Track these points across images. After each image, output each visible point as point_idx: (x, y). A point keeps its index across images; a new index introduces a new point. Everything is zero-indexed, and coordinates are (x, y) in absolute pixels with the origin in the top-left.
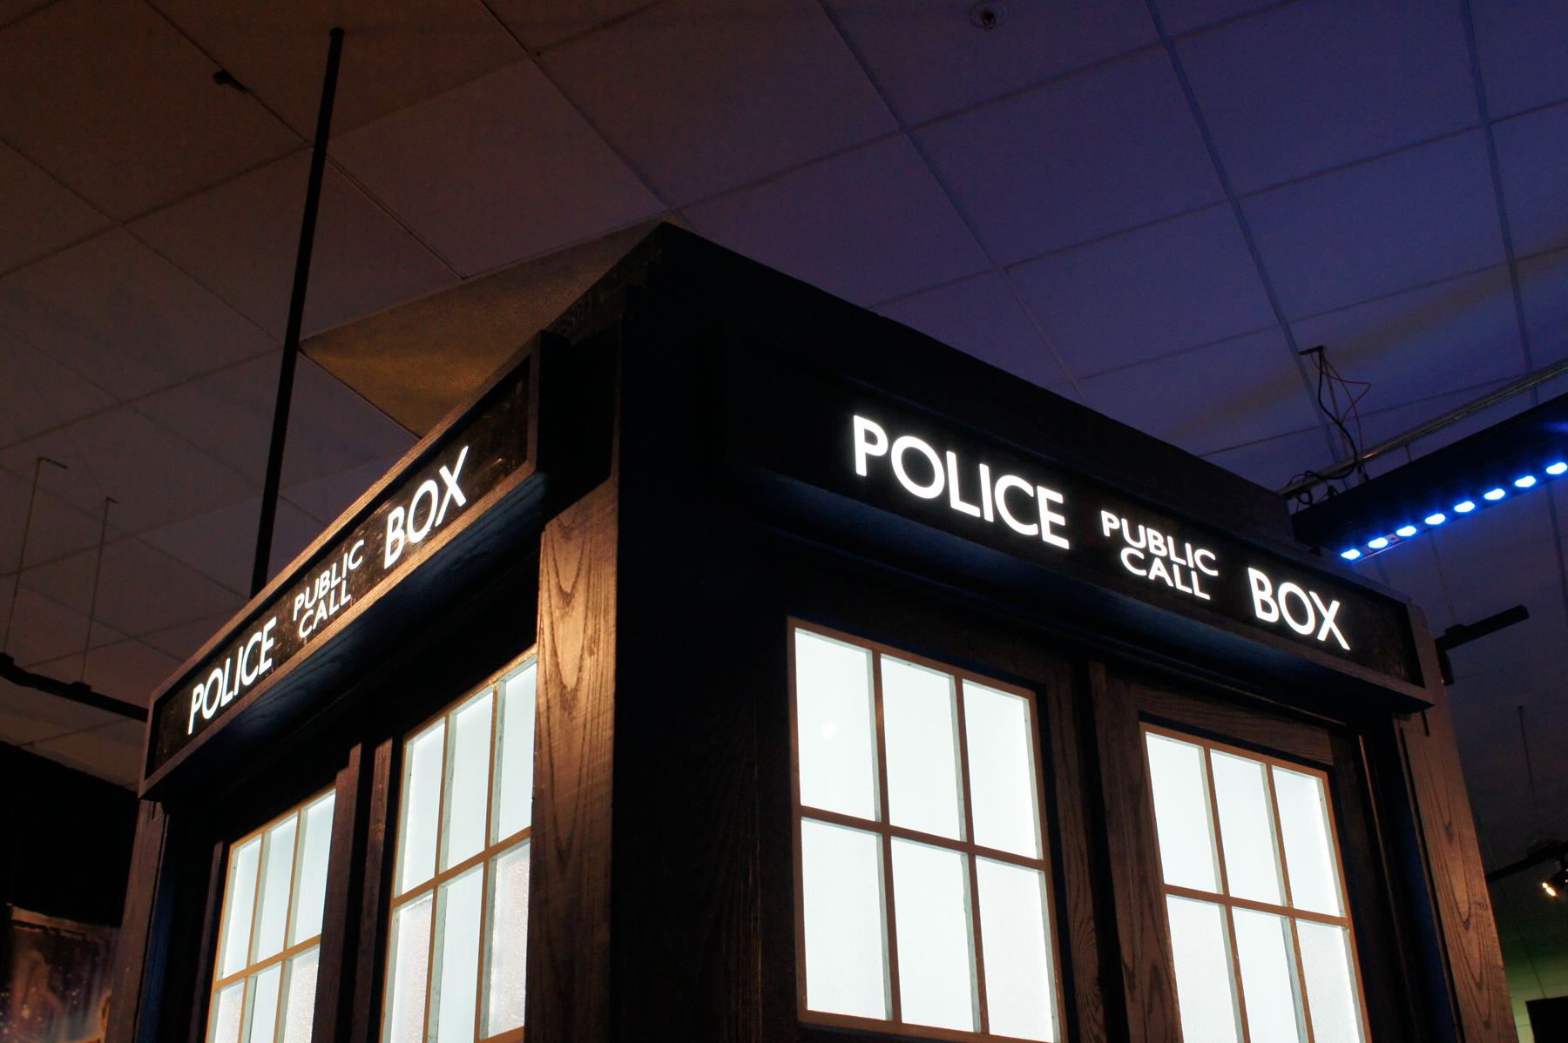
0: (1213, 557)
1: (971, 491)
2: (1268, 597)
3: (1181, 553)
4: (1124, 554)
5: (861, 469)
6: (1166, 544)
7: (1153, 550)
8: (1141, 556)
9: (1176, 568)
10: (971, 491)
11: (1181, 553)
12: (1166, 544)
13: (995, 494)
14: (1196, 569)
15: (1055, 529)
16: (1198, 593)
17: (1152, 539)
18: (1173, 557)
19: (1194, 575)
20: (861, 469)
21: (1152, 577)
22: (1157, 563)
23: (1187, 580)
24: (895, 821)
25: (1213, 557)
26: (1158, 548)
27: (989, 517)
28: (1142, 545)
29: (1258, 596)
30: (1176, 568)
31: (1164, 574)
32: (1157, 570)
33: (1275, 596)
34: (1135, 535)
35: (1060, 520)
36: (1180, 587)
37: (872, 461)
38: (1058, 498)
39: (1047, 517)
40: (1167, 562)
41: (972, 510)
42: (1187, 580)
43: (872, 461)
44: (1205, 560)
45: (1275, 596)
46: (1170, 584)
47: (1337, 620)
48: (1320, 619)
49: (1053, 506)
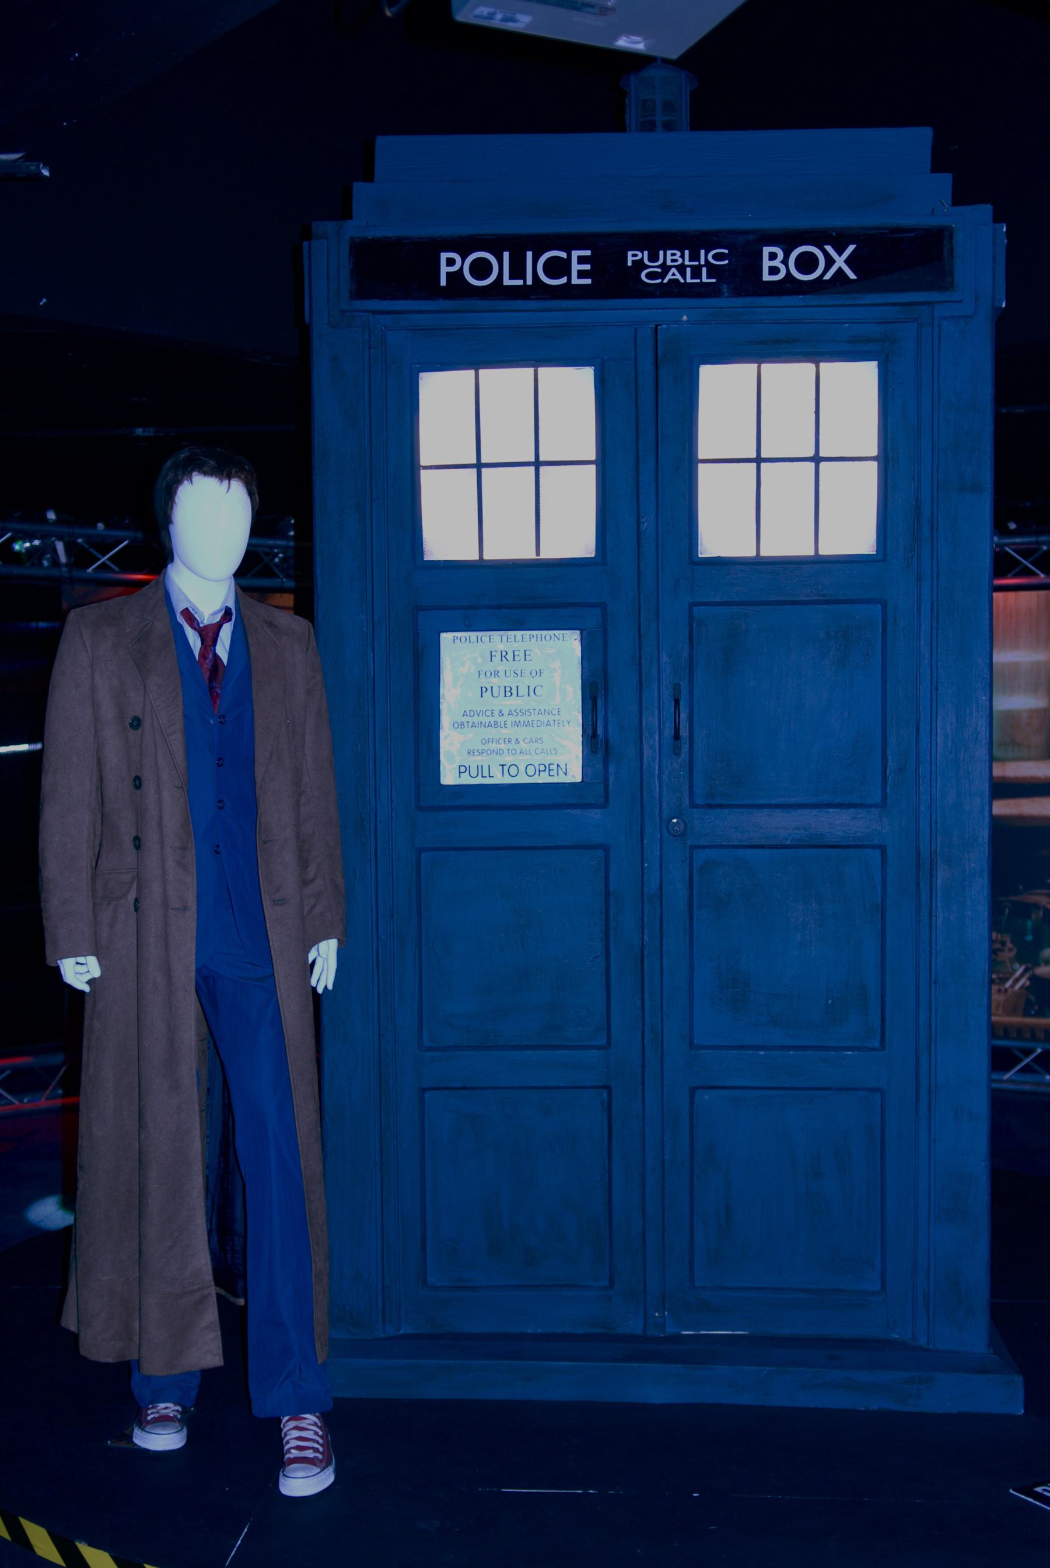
1: (517, 271)
3: (694, 257)
6: (683, 256)
7: (669, 263)
8: (659, 270)
9: (688, 270)
10: (517, 271)
11: (694, 257)
12: (683, 256)
13: (535, 267)
16: (705, 280)
17: (671, 256)
19: (704, 270)
21: (665, 281)
22: (674, 270)
23: (696, 272)
26: (673, 261)
27: (529, 282)
28: (661, 261)
29: (766, 264)
30: (688, 270)
31: (678, 276)
32: (673, 275)
33: (785, 262)
34: (653, 258)
36: (689, 280)
37: (448, 274)
38: (588, 253)
39: (575, 267)
40: (681, 269)
42: (696, 272)
43: (448, 274)
45: (785, 262)
46: (682, 281)
49: (581, 260)
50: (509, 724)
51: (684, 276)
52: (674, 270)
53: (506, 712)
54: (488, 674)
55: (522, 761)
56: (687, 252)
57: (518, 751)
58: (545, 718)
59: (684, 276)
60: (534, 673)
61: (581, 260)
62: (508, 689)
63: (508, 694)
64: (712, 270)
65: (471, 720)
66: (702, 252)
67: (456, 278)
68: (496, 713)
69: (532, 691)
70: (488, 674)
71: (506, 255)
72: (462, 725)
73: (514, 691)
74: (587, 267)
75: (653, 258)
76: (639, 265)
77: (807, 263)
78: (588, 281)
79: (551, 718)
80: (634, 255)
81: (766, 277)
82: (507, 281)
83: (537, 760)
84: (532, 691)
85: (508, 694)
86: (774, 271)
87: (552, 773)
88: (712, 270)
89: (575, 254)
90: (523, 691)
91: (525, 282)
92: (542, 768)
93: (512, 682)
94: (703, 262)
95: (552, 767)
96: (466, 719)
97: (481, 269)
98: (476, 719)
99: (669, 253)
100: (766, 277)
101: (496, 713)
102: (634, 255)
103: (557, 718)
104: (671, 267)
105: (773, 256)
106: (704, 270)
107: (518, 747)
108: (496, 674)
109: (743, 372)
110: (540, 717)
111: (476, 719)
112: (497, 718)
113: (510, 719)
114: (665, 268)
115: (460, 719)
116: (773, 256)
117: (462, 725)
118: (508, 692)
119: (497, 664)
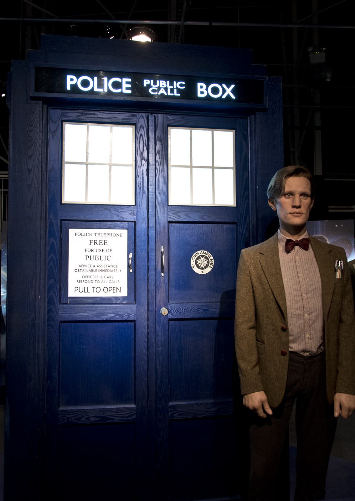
0: (184, 83)
1: (100, 85)
2: (203, 90)
3: (172, 84)
4: (150, 91)
5: (69, 88)
6: (166, 84)
7: (161, 86)
8: (157, 89)
9: (169, 90)
10: (100, 85)
12: (166, 84)
13: (108, 84)
14: (177, 88)
15: (127, 89)
17: (162, 83)
18: (169, 86)
19: (175, 90)
20: (69, 88)
21: (159, 94)
22: (162, 89)
24: (211, 170)
25: (184, 83)
27: (106, 90)
28: (157, 86)
29: (199, 90)
30: (169, 90)
32: (162, 91)
33: (207, 89)
34: (155, 83)
35: (129, 86)
36: (169, 94)
37: (72, 85)
38: (130, 80)
39: (125, 86)
40: (166, 89)
41: (101, 90)
43: (72, 85)
44: (181, 85)
45: (207, 89)
46: (166, 94)
47: (233, 91)
48: (224, 91)
49: (127, 83)
50: (97, 271)
51: (167, 92)
52: (162, 89)
53: (96, 266)
54: (89, 250)
55: (102, 286)
56: (168, 82)
57: (101, 281)
58: (111, 268)
59: (167, 92)
60: (108, 251)
61: (127, 83)
62: (97, 257)
63: (97, 259)
64: (179, 91)
65: (82, 269)
66: (175, 82)
67: (74, 87)
68: (92, 266)
69: (107, 258)
70: (89, 250)
71: (96, 78)
72: (79, 271)
73: (99, 258)
74: (129, 86)
75: (155, 83)
76: (149, 86)
77: (215, 91)
78: (130, 92)
79: (113, 269)
80: (147, 82)
81: (199, 95)
82: (96, 89)
83: (108, 285)
84: (107, 258)
85: (97, 259)
86: (202, 93)
87: (114, 291)
88: (179, 91)
89: (125, 80)
90: (103, 258)
91: (104, 90)
92: (110, 289)
93: (99, 254)
94: (175, 87)
95: (114, 289)
96: (80, 268)
97: (85, 83)
98: (84, 268)
99: (161, 81)
100: (199, 95)
101: (92, 266)
102: (147, 82)
103: (116, 269)
104: (161, 88)
105: (202, 87)
106: (175, 90)
107: (101, 280)
108: (92, 250)
109: (185, 132)
110: (109, 268)
111: (84, 268)
112: (93, 268)
113: (98, 269)
114: (159, 88)
115: (78, 268)
116: (202, 87)
117: (79, 271)
118: (97, 258)
119: (93, 246)
